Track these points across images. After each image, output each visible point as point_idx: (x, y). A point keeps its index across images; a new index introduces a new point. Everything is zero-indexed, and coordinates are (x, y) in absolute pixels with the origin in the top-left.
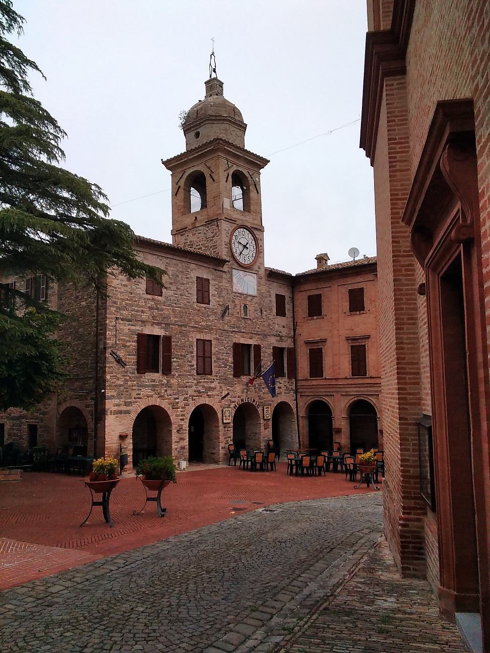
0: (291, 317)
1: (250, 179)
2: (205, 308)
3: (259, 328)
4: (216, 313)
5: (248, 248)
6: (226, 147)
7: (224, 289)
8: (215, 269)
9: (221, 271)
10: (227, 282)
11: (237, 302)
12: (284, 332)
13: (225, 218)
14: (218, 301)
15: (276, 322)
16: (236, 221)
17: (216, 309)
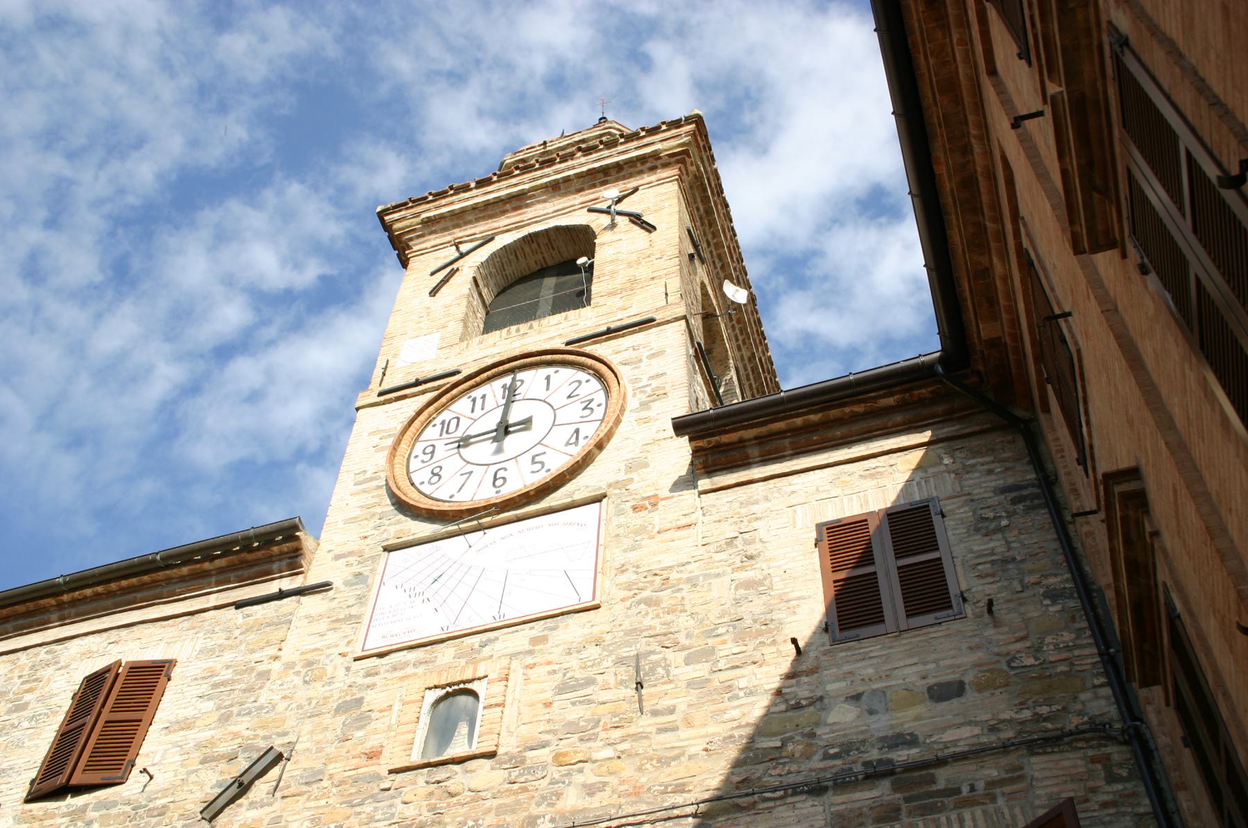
0: (1054, 595)
1: (598, 222)
2: (84, 809)
3: (591, 790)
4: (162, 811)
5: (526, 424)
6: (424, 216)
7: (290, 666)
8: (239, 605)
9: (281, 595)
10: (323, 626)
11: (373, 699)
12: (954, 729)
13: (380, 394)
14: (199, 746)
15: (830, 687)
16: (459, 372)
17: (165, 792)
